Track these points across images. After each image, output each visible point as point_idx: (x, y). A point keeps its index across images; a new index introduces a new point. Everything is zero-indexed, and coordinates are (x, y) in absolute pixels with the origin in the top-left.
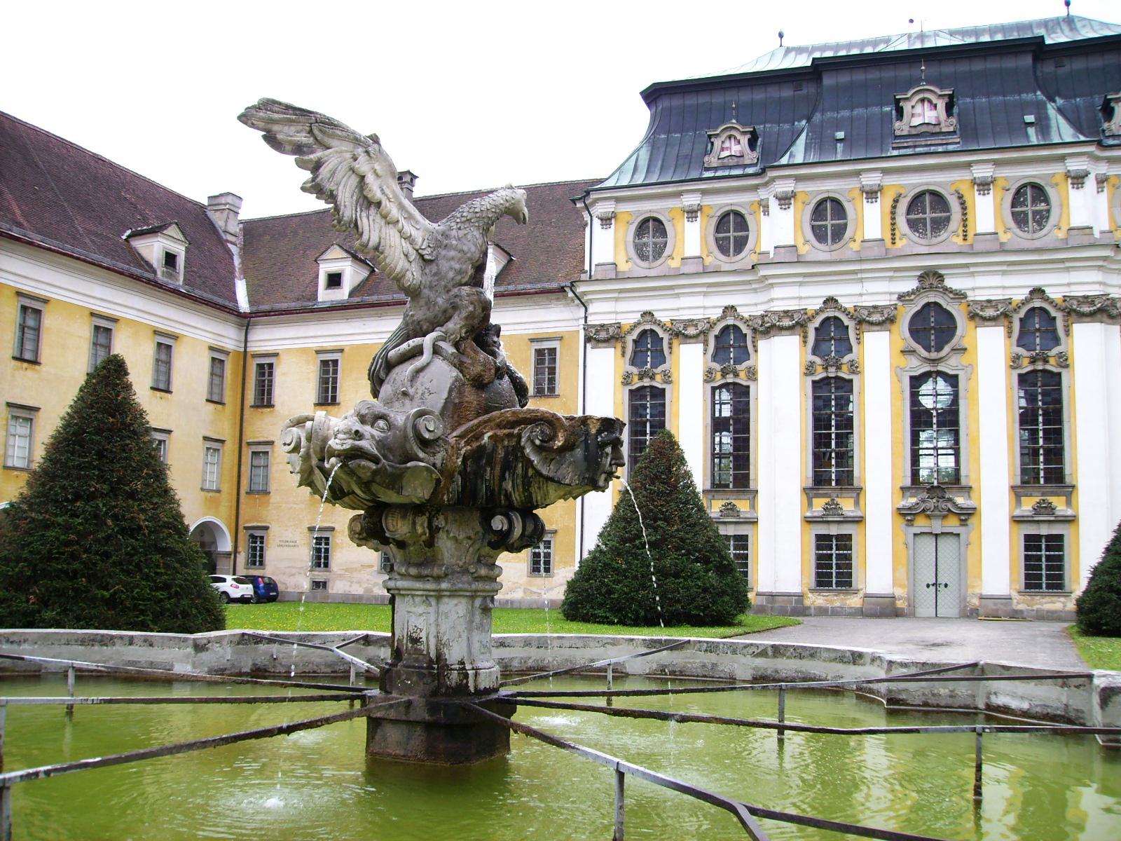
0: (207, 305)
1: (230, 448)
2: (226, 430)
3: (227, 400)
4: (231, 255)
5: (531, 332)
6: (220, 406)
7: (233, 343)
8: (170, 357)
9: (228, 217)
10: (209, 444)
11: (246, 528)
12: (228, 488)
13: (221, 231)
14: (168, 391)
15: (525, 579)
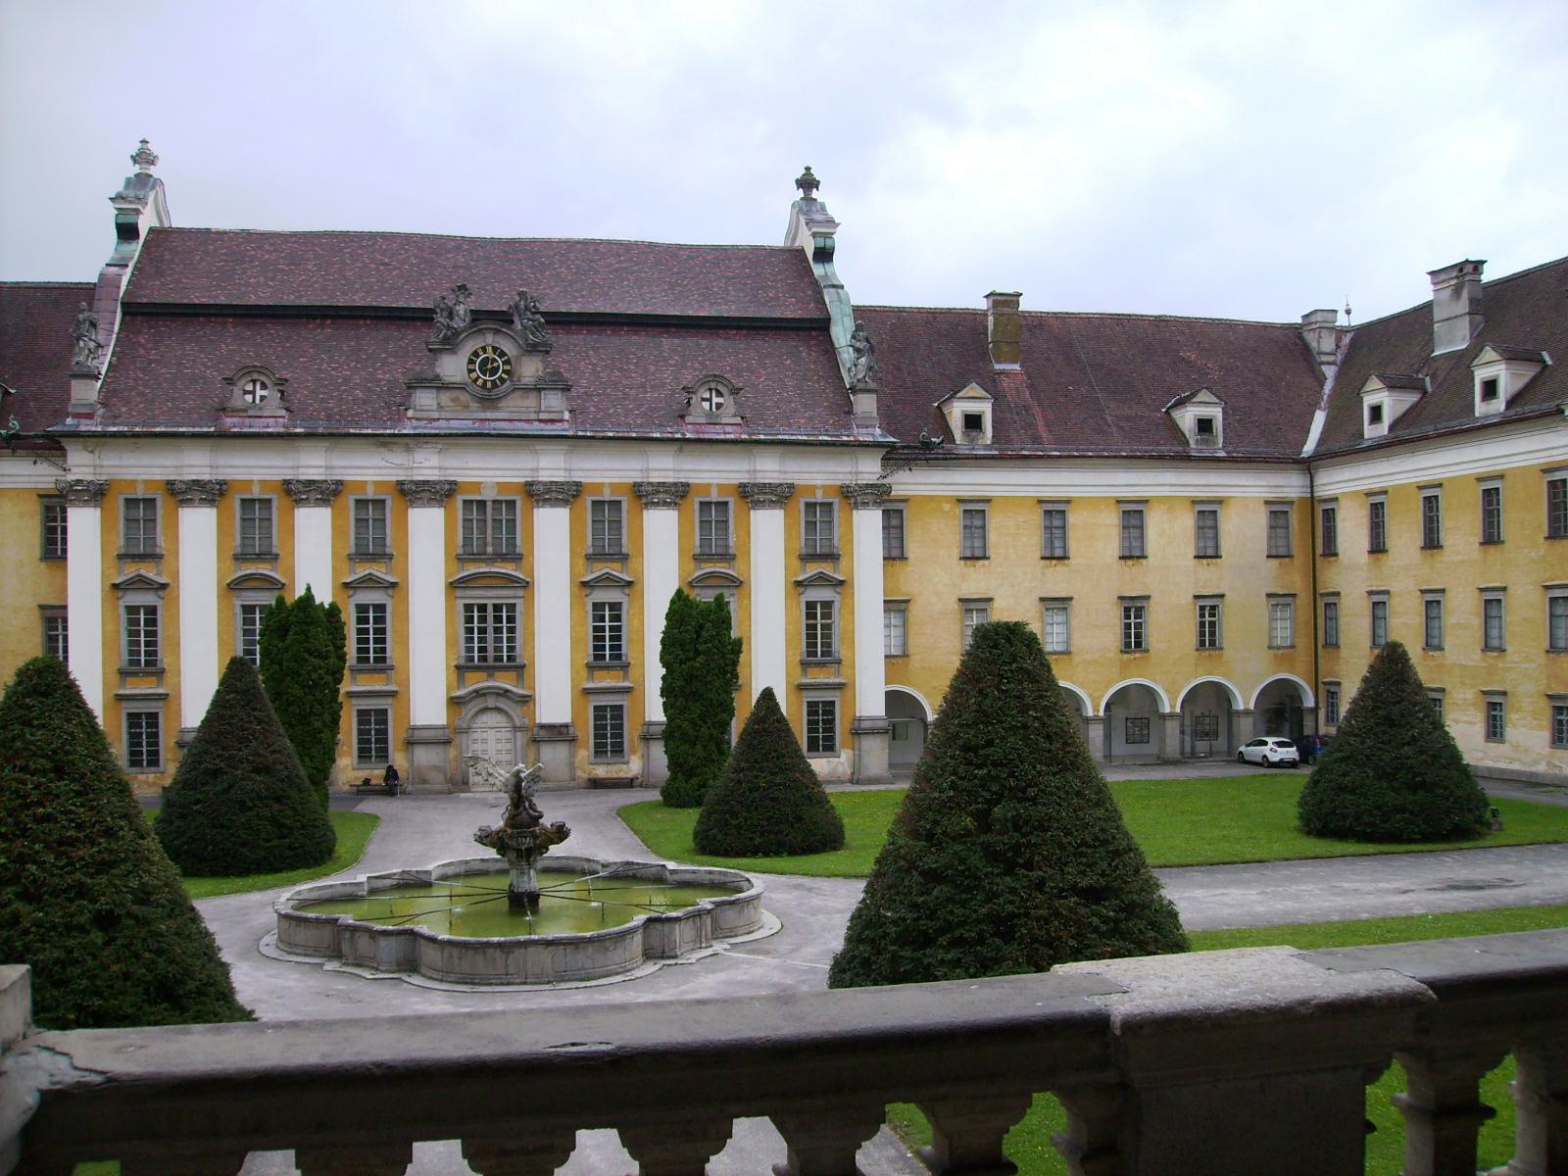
0: (1251, 462)
1: (1304, 599)
2: (1297, 582)
3: (1295, 551)
4: (1321, 380)
5: (1542, 461)
6: (1287, 560)
7: (1301, 490)
8: (1216, 521)
9: (1320, 337)
10: (1274, 601)
11: (1324, 683)
12: (1304, 644)
13: (1315, 353)
14: (1217, 556)
15: (1547, 750)
